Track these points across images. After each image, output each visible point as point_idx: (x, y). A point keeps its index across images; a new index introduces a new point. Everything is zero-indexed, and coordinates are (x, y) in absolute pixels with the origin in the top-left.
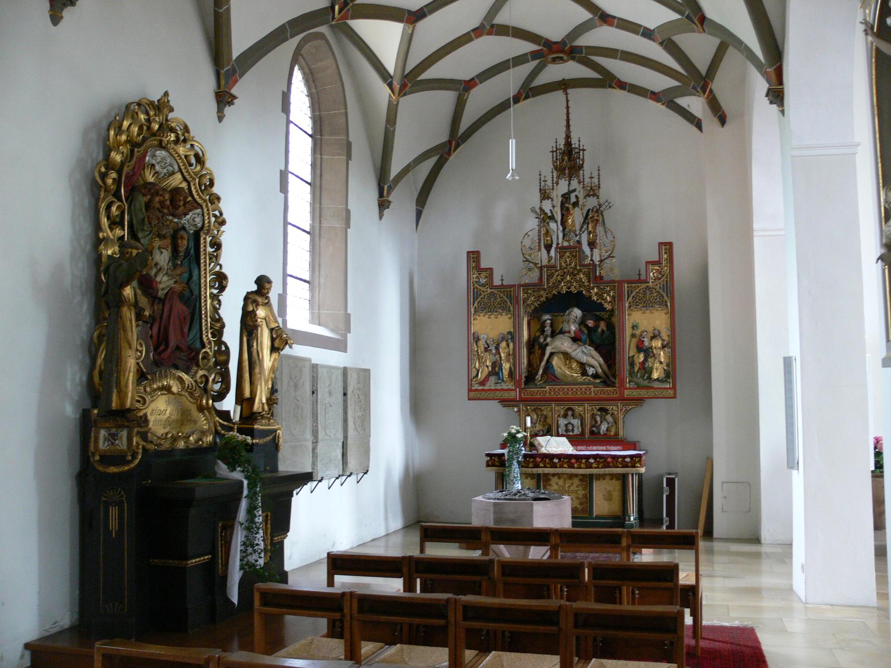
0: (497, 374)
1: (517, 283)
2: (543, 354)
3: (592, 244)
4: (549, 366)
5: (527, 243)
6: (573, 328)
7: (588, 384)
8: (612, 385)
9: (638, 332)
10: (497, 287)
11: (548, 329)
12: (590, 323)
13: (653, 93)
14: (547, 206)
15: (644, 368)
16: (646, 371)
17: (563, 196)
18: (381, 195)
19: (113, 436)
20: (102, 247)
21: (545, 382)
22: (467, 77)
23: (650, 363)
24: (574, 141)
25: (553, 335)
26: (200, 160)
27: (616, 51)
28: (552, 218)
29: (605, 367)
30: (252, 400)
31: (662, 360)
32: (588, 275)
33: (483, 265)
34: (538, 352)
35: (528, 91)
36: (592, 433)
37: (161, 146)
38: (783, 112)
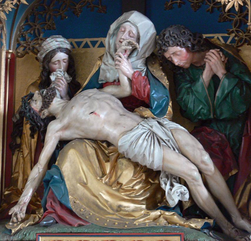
6: (127, 68)
11: (60, 77)
12: (178, 55)
21: (37, 224)
25: (73, 90)
29: (219, 183)
34: (28, 141)
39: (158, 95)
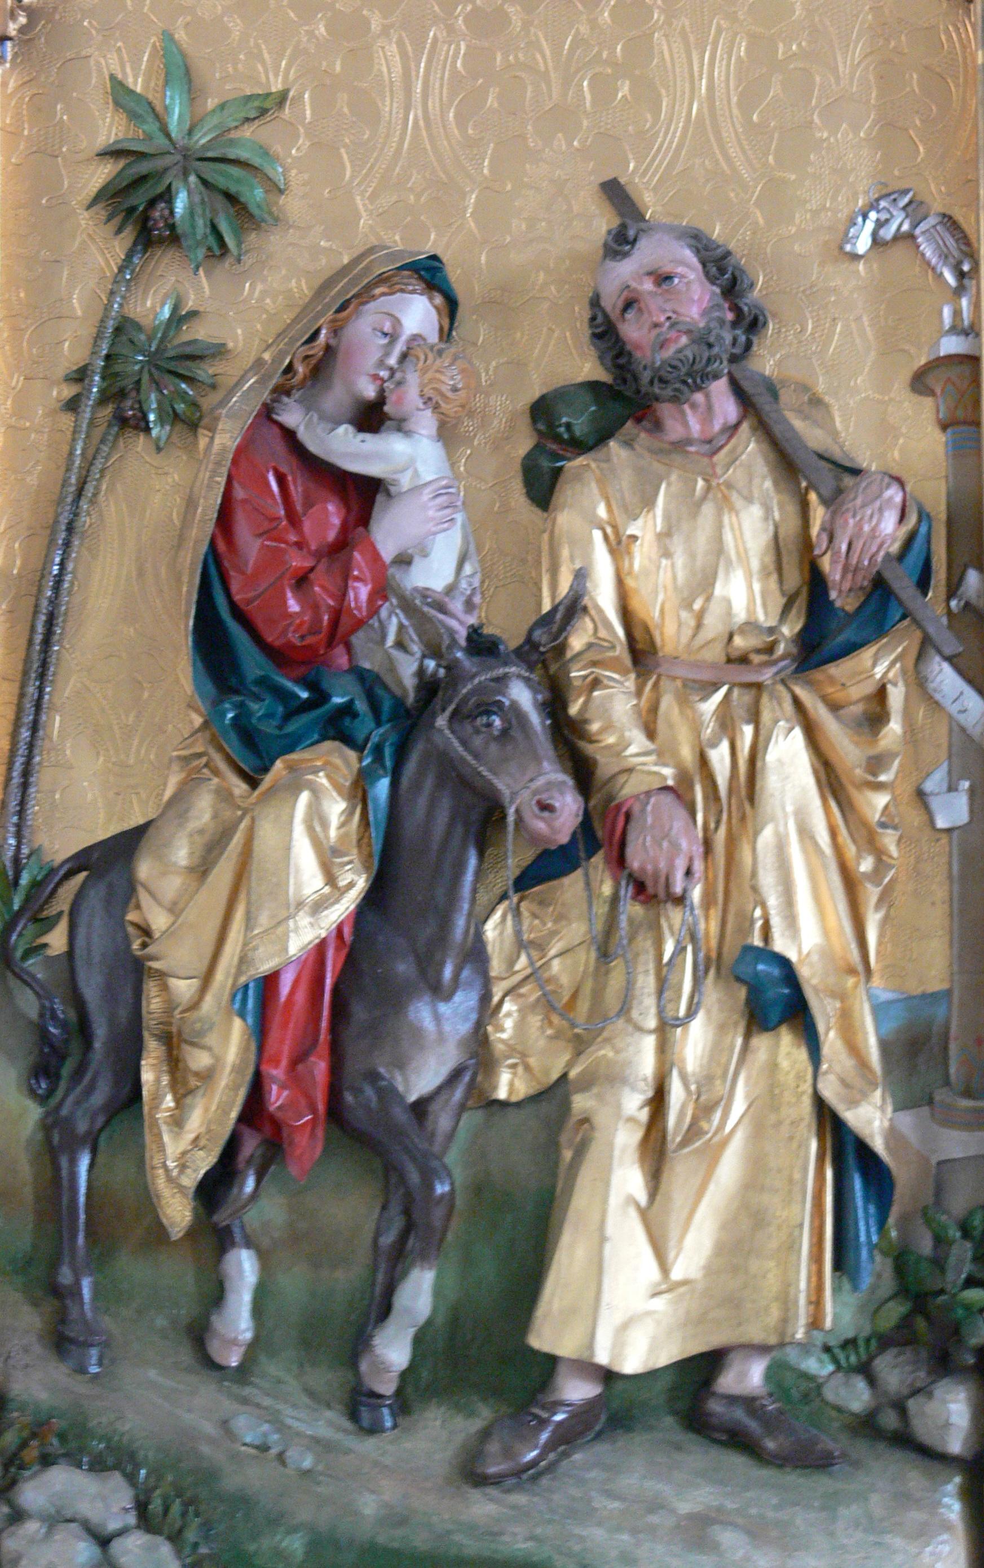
9: (243, 312)
15: (370, 1134)
16: (412, 1192)
23: (507, 997)
31: (807, 933)
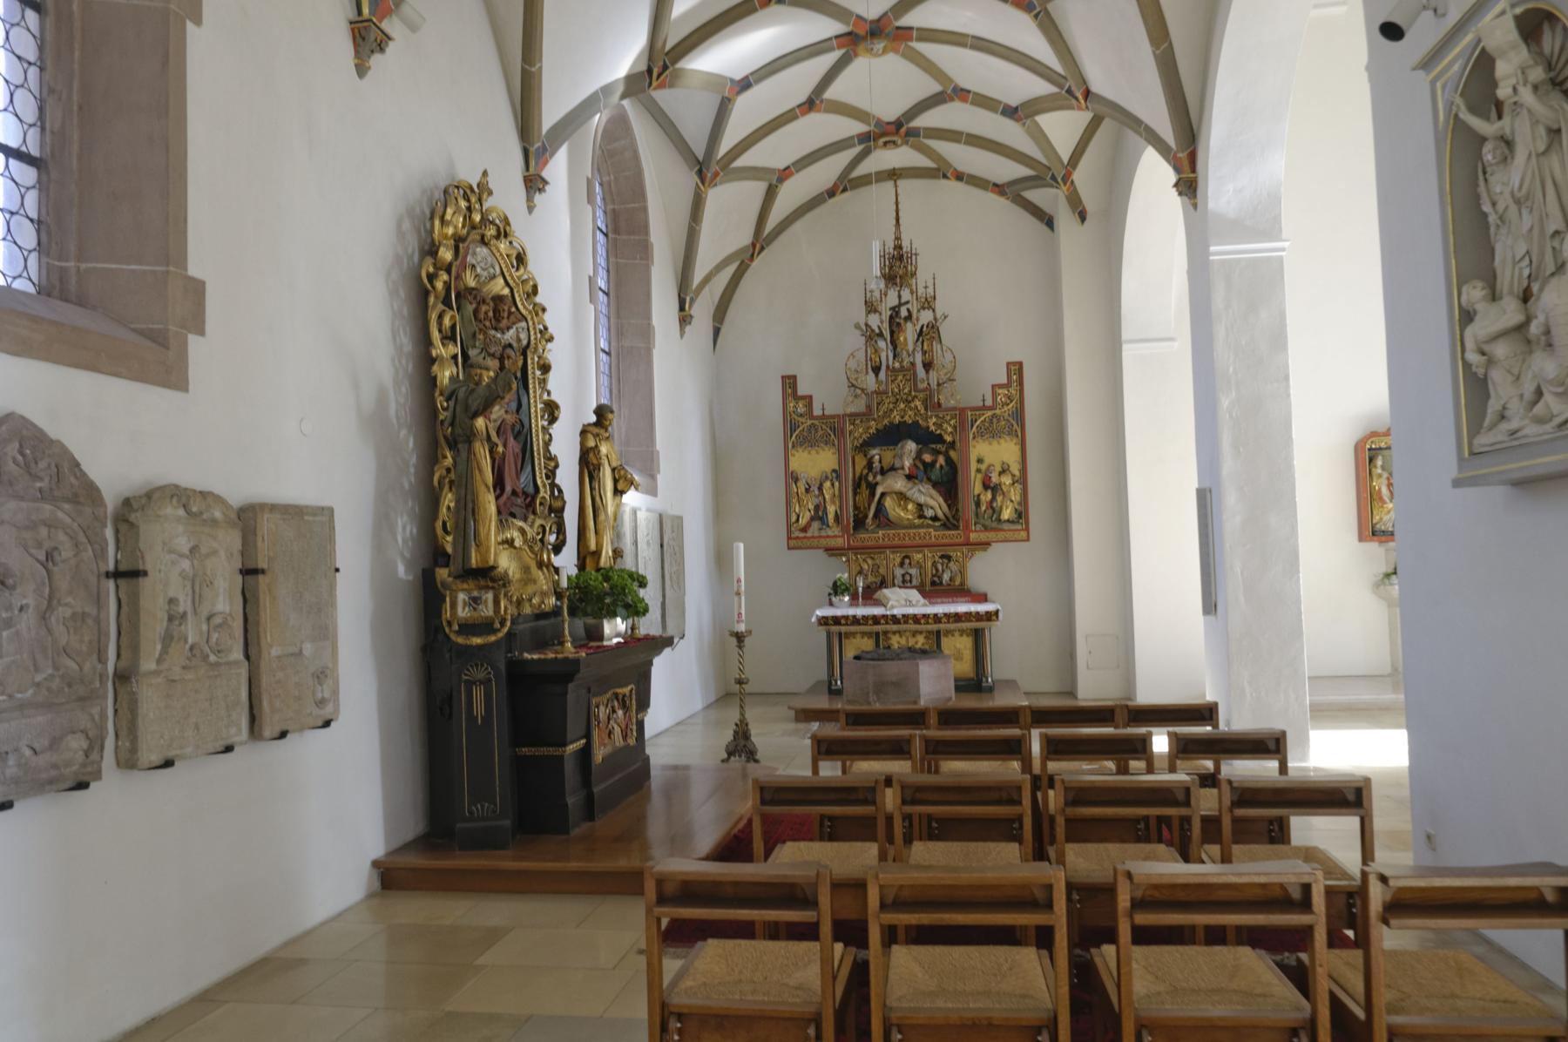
0: (821, 519)
1: (841, 412)
2: (873, 494)
3: (928, 366)
4: (880, 509)
5: (852, 364)
6: (907, 464)
7: (928, 526)
8: (956, 527)
10: (817, 418)
11: (876, 465)
13: (995, 185)
14: (874, 321)
16: (995, 511)
17: (893, 309)
18: (682, 309)
19: (475, 601)
20: (435, 368)
22: (781, 164)
24: (905, 244)
26: (521, 259)
27: (960, 133)
28: (881, 335)
30: (597, 554)
32: (924, 402)
33: (800, 392)
35: (846, 183)
36: (933, 583)
37: (483, 241)
38: (1195, 206)
39: (921, 474)
